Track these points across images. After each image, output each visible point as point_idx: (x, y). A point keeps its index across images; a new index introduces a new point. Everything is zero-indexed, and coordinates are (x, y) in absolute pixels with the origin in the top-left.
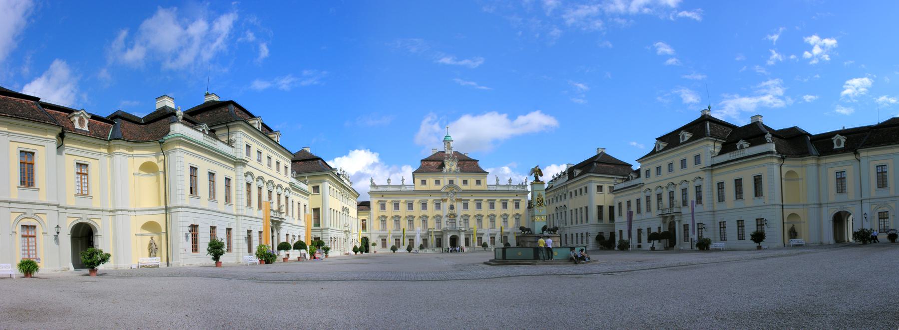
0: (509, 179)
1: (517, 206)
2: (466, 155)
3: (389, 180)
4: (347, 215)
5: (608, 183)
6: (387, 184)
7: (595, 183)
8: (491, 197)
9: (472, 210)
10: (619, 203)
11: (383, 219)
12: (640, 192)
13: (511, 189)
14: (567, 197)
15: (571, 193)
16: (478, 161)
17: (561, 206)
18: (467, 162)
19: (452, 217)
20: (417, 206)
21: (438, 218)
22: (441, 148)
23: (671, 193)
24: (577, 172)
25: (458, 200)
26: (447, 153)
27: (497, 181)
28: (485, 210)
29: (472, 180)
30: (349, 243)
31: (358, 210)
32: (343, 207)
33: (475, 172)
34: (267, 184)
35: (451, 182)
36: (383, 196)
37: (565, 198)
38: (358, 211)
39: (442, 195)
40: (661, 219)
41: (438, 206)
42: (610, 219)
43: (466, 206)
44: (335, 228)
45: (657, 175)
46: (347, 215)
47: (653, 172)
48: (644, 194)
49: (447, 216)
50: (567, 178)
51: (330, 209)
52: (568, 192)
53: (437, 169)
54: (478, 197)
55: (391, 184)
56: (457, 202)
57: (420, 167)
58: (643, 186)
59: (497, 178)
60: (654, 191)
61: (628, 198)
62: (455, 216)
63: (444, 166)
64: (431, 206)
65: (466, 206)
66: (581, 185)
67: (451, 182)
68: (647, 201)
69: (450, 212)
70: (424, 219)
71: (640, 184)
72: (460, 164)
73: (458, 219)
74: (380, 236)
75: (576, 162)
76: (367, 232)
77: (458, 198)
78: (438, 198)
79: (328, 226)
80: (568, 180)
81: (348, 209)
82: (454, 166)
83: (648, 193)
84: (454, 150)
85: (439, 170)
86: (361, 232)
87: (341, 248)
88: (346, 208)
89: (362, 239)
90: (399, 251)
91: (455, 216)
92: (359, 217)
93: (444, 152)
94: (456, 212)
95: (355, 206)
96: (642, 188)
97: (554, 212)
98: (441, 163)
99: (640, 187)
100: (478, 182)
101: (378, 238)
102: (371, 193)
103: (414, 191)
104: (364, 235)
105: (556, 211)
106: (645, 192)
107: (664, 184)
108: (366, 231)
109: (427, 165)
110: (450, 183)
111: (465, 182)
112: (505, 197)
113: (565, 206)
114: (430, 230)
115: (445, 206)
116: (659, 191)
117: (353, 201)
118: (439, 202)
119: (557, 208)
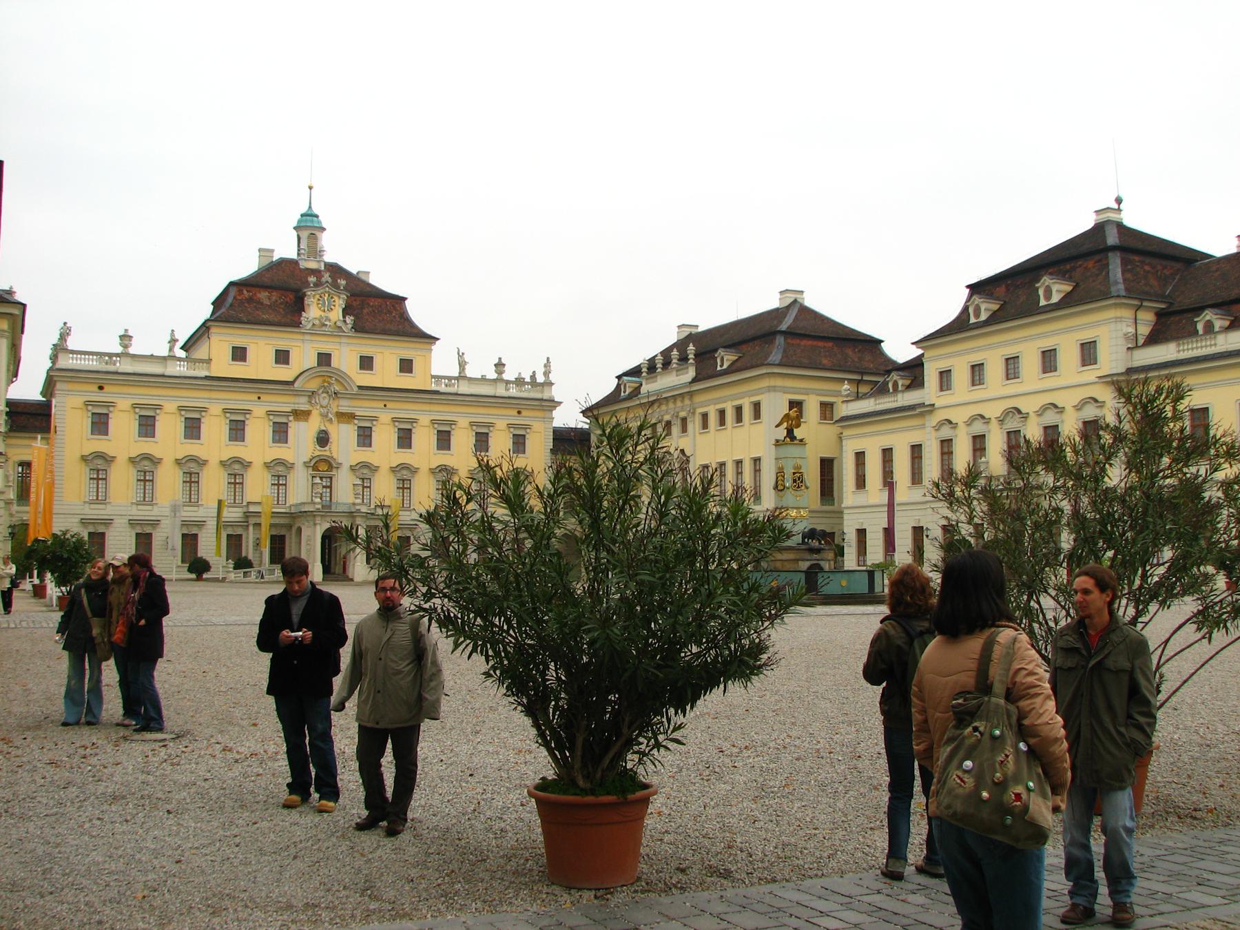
0: (497, 361)
1: (519, 443)
2: (363, 277)
3: (125, 338)
5: (819, 393)
6: (119, 350)
7: (818, 395)
8: (444, 412)
10: (857, 454)
11: (98, 465)
12: (923, 427)
13: (501, 391)
14: (690, 427)
15: (705, 416)
16: (406, 299)
19: (323, 467)
20: (215, 429)
21: (279, 471)
22: (286, 248)
23: (1012, 436)
24: (726, 358)
25: (351, 417)
26: (304, 265)
27: (462, 365)
29: (387, 355)
35: (324, 359)
36: (101, 388)
37: (684, 429)
39: (297, 400)
41: (280, 433)
42: (823, 494)
43: (365, 437)
45: (973, 385)
47: (961, 376)
48: (934, 434)
50: (691, 373)
52: (694, 413)
54: (405, 410)
55: (132, 351)
56: (339, 422)
58: (931, 412)
59: (461, 356)
60: (962, 426)
61: (886, 441)
62: (331, 467)
64: (259, 431)
65: (365, 437)
67: (324, 359)
68: (943, 454)
69: (317, 453)
70: (236, 470)
71: (923, 405)
75: (706, 322)
77: (344, 410)
78: (284, 403)
80: (690, 383)
83: (946, 432)
84: (329, 258)
91: (331, 467)
96: (927, 417)
99: (922, 415)
100: (406, 366)
103: (207, 378)
106: (938, 427)
107: (993, 411)
109: (250, 300)
110: (319, 364)
112: (482, 415)
113: (682, 451)
114: (252, 509)
115: (303, 436)
116: (978, 428)
118: (283, 420)
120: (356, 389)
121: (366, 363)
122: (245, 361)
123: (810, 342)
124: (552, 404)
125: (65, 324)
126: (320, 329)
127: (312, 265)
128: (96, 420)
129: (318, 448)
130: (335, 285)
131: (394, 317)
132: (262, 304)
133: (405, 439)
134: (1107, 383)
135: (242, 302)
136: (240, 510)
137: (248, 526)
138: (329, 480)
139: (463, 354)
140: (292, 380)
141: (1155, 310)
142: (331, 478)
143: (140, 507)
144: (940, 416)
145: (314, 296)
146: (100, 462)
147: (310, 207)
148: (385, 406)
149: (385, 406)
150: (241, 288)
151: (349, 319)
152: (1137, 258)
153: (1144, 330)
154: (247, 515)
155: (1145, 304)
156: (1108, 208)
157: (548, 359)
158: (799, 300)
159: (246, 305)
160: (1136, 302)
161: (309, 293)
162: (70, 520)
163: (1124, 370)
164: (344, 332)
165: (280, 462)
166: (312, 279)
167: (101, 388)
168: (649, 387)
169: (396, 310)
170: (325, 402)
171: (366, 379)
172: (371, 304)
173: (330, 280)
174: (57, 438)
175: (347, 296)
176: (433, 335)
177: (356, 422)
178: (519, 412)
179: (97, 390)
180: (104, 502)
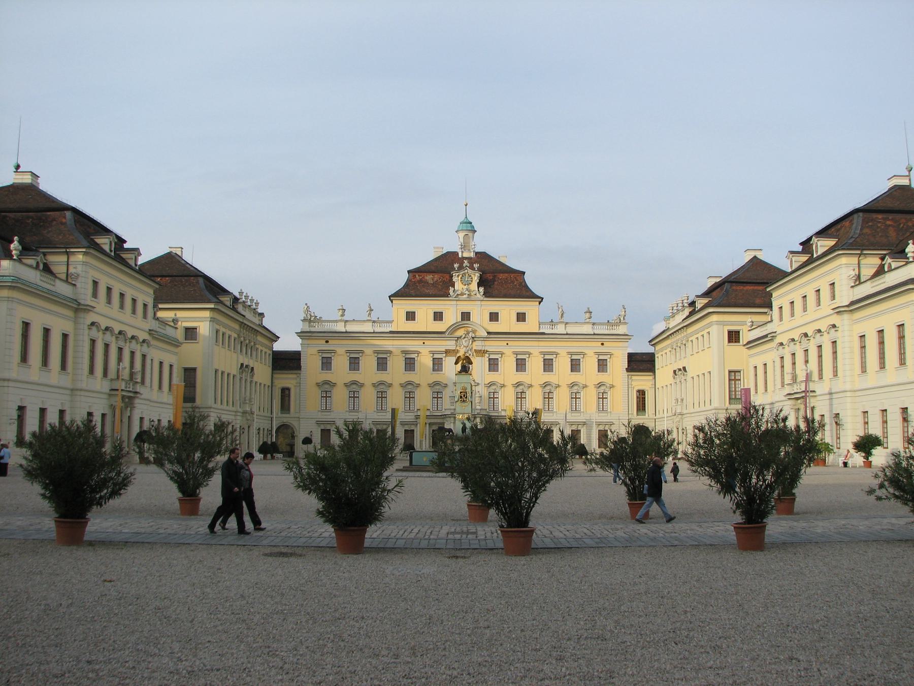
1: (602, 365)
4: (249, 380)
9: (507, 371)
12: (771, 349)
15: (692, 341)
17: (680, 370)
18: (501, 276)
22: (452, 243)
28: (535, 371)
29: (508, 309)
32: (242, 365)
34: (117, 338)
35: (466, 316)
36: (327, 342)
40: (790, 402)
43: (493, 365)
44: (225, 407)
50: (687, 312)
51: (216, 371)
55: (345, 318)
57: (407, 285)
65: (493, 365)
66: (702, 329)
67: (466, 316)
74: (318, 423)
79: (210, 402)
81: (253, 368)
84: (479, 249)
88: (247, 366)
93: (456, 254)
97: (672, 381)
102: (302, 334)
103: (391, 332)
105: (674, 378)
109: (420, 281)
111: (494, 317)
112: (576, 346)
113: (684, 368)
119: (675, 371)
122: (414, 320)
123: (752, 287)
125: (306, 304)
127: (466, 255)
128: (325, 361)
130: (473, 269)
133: (521, 365)
134: (838, 313)
136: (412, 414)
141: (880, 256)
144: (778, 340)
145: (458, 276)
146: (327, 386)
147: (466, 217)
148: (507, 344)
149: (507, 344)
150: (415, 274)
151: (482, 289)
152: (880, 216)
153: (867, 272)
154: (417, 417)
155: (865, 252)
156: (895, 176)
158: (758, 257)
159: (417, 284)
160: (859, 252)
163: (847, 304)
166: (456, 266)
167: (327, 342)
168: (673, 323)
170: (465, 344)
171: (494, 327)
173: (468, 265)
178: (602, 344)
179: (324, 343)
180: (330, 411)
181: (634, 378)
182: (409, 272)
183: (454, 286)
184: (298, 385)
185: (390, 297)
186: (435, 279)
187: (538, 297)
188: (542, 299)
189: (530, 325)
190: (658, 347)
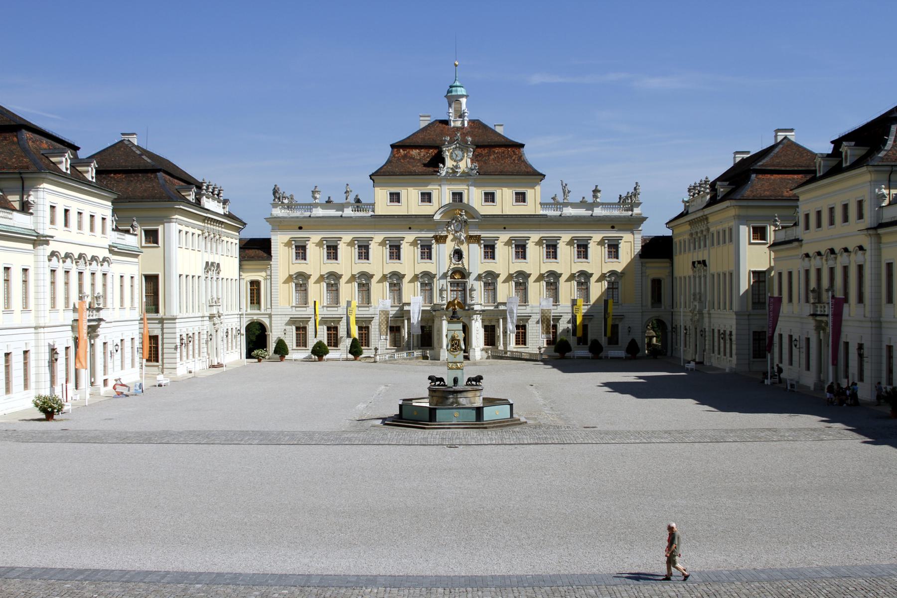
0: (594, 189)
11: (301, 281)
16: (522, 146)
18: (497, 150)
19: (459, 276)
25: (477, 239)
27: (566, 192)
30: (219, 339)
31: (243, 259)
33: (512, 174)
35: (458, 196)
36: (300, 228)
38: (240, 261)
41: (426, 252)
43: (490, 251)
46: (215, 278)
49: (445, 276)
53: (425, 165)
56: (469, 243)
57: (389, 162)
63: (443, 161)
65: (490, 251)
67: (458, 196)
69: (452, 266)
72: (480, 155)
73: (471, 282)
74: (292, 321)
76: (263, 311)
77: (472, 233)
82: (464, 161)
85: (431, 169)
86: (249, 311)
87: (202, 354)
89: (249, 328)
90: (332, 354)
92: (244, 275)
94: (466, 267)
95: (235, 250)
98: (436, 151)
101: (287, 324)
103: (371, 216)
104: (255, 317)
108: (259, 309)
109: (405, 157)
114: (406, 308)
117: (230, 240)
120: (481, 217)
121: (490, 197)
124: (641, 220)
126: (453, 176)
129: (453, 261)
131: (514, 160)
132: (414, 159)
135: (399, 159)
137: (403, 320)
138: (463, 285)
139: (566, 185)
140: (433, 214)
142: (465, 284)
143: (329, 309)
157: (636, 183)
161: (444, 149)
162: (283, 319)
164: (471, 176)
165: (426, 274)
169: (515, 154)
172: (496, 151)
174: (273, 262)
175: (473, 149)
176: (540, 171)
177: (482, 242)
181: (648, 265)
182: (393, 146)
183: (444, 164)
184: (269, 277)
185: (370, 176)
186: (422, 154)
187: (541, 175)
188: (544, 176)
189: (531, 207)
190: (677, 231)
